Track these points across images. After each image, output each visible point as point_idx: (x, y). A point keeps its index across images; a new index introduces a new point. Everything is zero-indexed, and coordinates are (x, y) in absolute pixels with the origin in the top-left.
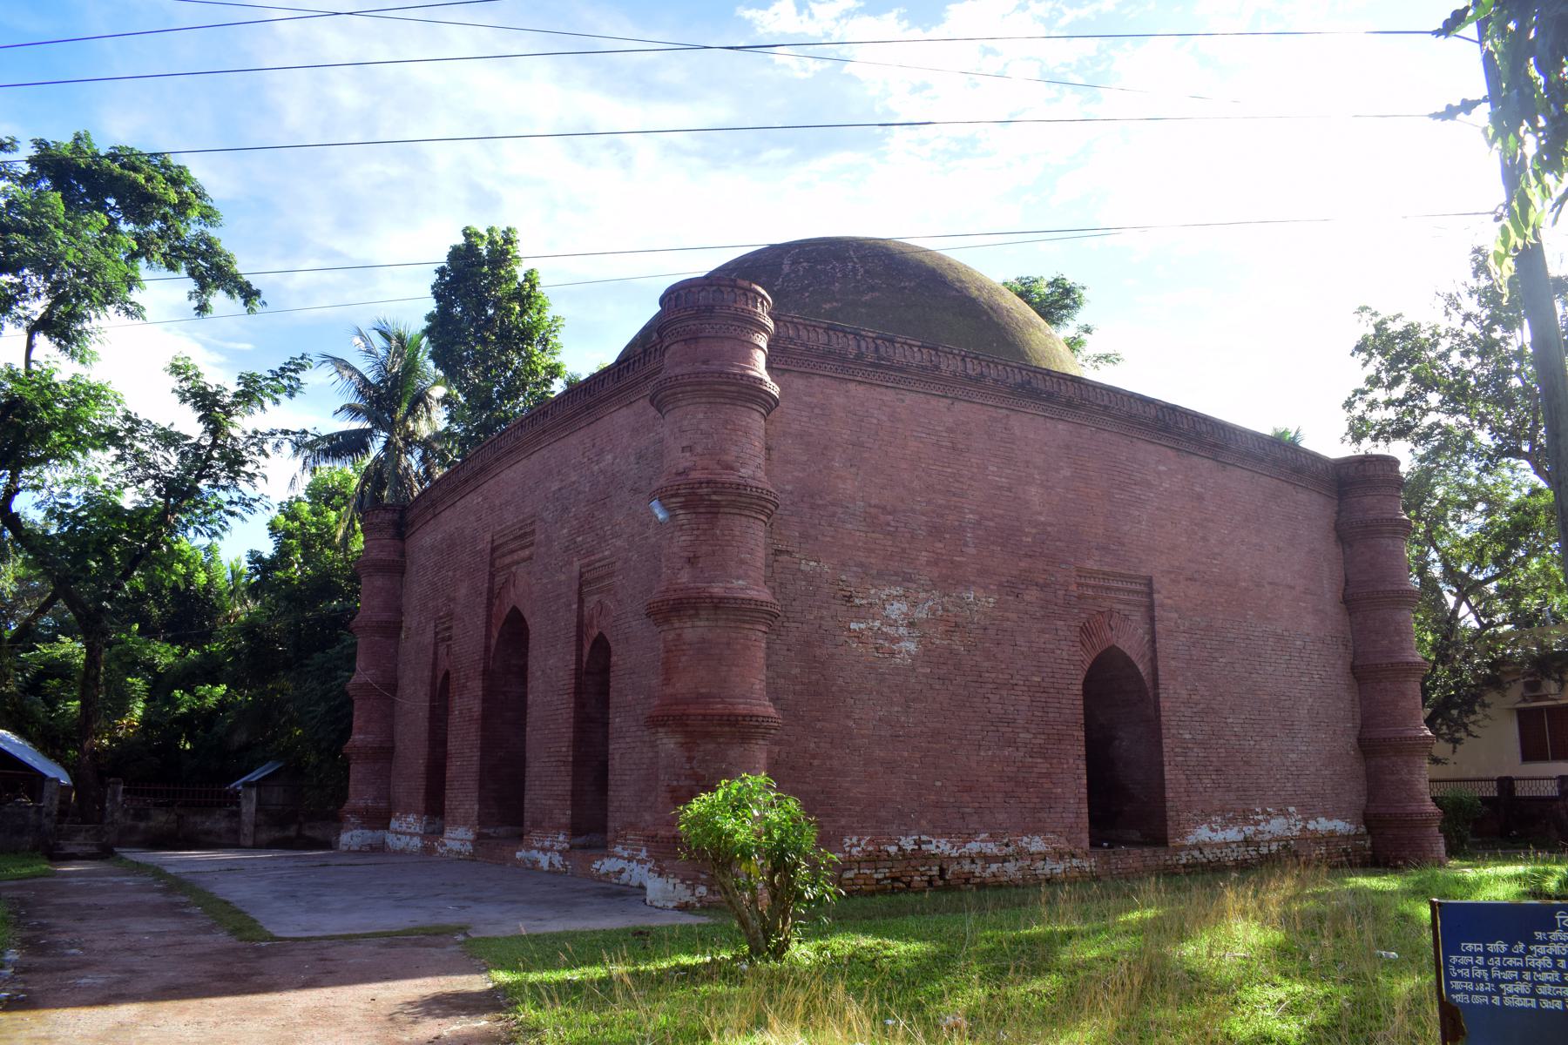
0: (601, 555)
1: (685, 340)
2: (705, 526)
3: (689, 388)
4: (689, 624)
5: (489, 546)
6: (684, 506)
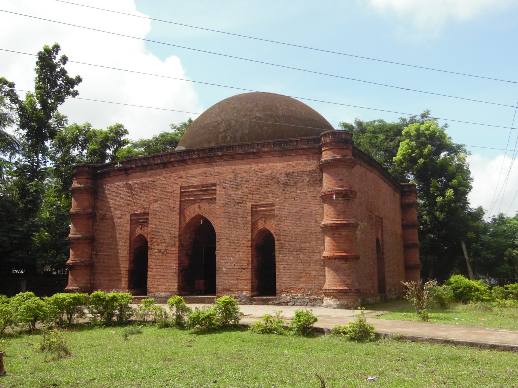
0: (266, 203)
1: (339, 148)
2: (347, 203)
3: (343, 163)
4: (344, 230)
5: (179, 191)
6: (342, 197)
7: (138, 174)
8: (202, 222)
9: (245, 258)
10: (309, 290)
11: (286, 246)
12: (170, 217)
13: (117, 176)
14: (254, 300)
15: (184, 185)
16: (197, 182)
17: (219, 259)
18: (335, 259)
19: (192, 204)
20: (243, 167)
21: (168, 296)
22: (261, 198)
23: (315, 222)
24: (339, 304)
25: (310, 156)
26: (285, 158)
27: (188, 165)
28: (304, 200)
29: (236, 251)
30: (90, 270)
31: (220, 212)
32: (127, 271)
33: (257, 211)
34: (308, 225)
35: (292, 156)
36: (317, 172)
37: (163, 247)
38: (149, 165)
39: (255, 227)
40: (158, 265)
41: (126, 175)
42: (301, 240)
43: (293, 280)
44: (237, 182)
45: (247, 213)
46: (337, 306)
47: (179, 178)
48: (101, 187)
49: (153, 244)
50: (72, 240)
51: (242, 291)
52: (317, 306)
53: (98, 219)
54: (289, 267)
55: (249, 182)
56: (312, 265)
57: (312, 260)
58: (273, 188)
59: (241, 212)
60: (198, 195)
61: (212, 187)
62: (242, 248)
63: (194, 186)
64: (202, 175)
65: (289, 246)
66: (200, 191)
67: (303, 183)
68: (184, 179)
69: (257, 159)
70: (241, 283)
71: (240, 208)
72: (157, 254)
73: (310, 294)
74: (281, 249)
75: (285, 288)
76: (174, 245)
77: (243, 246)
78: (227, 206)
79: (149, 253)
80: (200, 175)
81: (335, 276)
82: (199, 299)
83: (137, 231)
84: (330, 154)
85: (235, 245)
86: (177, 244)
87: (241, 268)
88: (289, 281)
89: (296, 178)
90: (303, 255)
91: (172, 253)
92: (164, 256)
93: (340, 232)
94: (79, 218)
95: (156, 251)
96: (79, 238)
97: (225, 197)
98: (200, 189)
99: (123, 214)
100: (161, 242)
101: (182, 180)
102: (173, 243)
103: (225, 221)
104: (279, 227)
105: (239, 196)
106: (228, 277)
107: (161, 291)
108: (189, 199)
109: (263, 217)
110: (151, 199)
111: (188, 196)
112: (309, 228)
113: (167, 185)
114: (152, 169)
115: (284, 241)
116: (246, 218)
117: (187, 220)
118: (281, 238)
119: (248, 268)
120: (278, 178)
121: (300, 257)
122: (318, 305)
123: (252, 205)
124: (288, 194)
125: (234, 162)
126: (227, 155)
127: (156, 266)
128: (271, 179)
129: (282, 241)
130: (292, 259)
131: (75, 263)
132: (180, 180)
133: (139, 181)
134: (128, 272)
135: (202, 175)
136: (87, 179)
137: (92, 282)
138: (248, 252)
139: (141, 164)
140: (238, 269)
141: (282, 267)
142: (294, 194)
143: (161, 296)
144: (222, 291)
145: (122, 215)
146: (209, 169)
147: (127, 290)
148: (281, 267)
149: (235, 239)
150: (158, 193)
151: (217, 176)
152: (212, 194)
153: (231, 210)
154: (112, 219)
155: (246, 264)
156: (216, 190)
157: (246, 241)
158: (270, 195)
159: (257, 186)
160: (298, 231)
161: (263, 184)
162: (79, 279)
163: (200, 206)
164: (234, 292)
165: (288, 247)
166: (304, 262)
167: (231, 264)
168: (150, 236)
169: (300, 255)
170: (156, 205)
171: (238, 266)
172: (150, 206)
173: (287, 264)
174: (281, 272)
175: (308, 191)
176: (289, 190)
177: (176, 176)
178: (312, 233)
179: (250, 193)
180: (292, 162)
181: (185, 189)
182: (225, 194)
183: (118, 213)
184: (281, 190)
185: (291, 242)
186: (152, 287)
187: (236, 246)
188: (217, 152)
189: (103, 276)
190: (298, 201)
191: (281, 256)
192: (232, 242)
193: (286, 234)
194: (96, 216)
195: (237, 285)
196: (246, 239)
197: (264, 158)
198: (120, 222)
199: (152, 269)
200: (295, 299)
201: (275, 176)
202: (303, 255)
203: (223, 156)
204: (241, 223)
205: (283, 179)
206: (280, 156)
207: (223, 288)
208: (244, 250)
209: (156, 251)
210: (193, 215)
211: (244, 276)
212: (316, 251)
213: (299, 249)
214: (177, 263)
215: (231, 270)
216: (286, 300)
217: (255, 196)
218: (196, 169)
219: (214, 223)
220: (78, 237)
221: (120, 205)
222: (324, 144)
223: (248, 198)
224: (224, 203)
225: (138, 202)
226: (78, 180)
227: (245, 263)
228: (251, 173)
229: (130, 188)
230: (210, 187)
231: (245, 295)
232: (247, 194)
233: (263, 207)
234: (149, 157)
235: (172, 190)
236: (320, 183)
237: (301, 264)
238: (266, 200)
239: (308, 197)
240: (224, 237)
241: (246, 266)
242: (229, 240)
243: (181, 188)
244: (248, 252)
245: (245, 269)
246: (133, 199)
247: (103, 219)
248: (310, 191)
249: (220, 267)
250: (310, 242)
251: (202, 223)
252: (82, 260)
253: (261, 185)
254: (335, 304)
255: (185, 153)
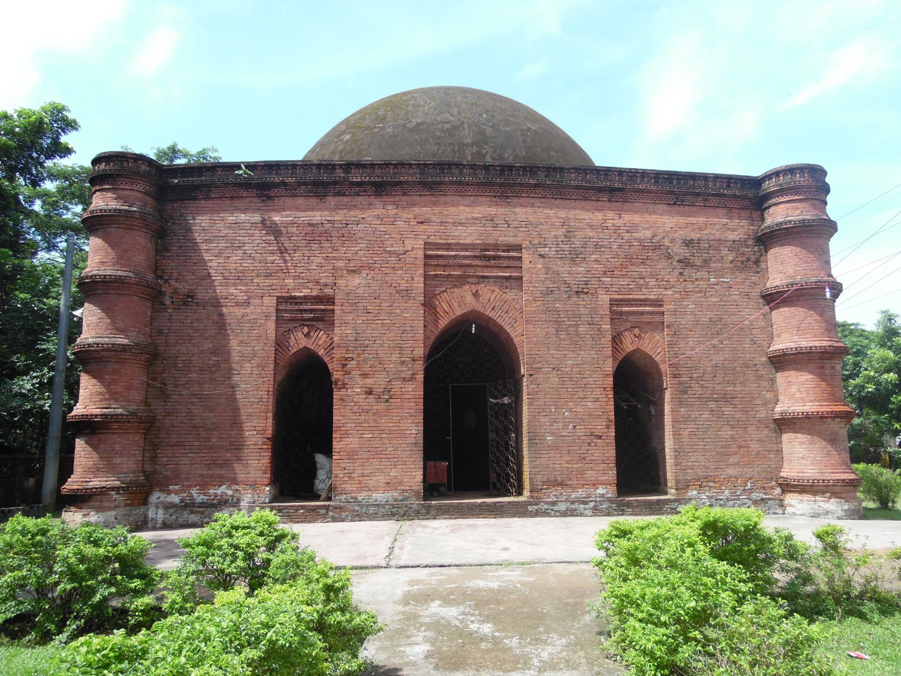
5: (420, 254)
7: (300, 201)
8: (473, 329)
9: (601, 413)
10: (747, 481)
11: (694, 389)
12: (398, 311)
13: (232, 198)
14: (629, 504)
15: (433, 239)
16: (470, 238)
17: (535, 414)
18: (834, 418)
19: (455, 286)
20: (587, 217)
21: (395, 500)
22: (631, 287)
23: (752, 342)
24: (849, 509)
25: (734, 210)
26: (682, 209)
27: (446, 195)
28: (725, 298)
29: (577, 396)
30: (143, 436)
31: (534, 309)
32: (268, 438)
33: (621, 313)
34: (738, 349)
35: (695, 209)
36: (749, 245)
37: (378, 382)
38: (335, 183)
39: (617, 347)
40: (365, 425)
41: (263, 201)
42: (726, 379)
43: (712, 460)
44: (573, 246)
45: (600, 316)
46: (844, 513)
47: (422, 223)
48: (177, 222)
49: (348, 373)
50: (103, 351)
51: (595, 485)
52: (769, 513)
53: (168, 302)
54: (701, 433)
55: (603, 249)
56: (751, 429)
57: (750, 419)
58: (659, 266)
59: (587, 312)
60: (472, 266)
61: (508, 251)
62: (591, 390)
63: (462, 244)
64: (483, 222)
65: (700, 389)
66: (476, 257)
67: (721, 263)
68: (435, 227)
69: (619, 204)
70: (591, 469)
71: (584, 303)
72: (361, 399)
73: (749, 489)
74: (682, 396)
75: (694, 477)
76: (412, 379)
77: (594, 386)
78: (550, 298)
79: (335, 397)
80: (477, 222)
81: (832, 453)
82: (487, 505)
83: (292, 337)
84: (807, 209)
85: (574, 383)
86: (420, 377)
87: (592, 434)
88: (703, 463)
89: (706, 251)
90: (731, 409)
91: (408, 397)
92: (384, 404)
93: (833, 365)
94: (121, 294)
95: (358, 390)
96: (124, 348)
97: (546, 276)
98: (477, 254)
99: (253, 294)
100: (374, 369)
101: (427, 227)
102: (407, 374)
103: (546, 330)
104: (677, 349)
105: (580, 277)
106: (559, 455)
107: (376, 490)
108: (449, 275)
109: (635, 327)
110: (341, 264)
111: (444, 266)
112: (739, 355)
113: (386, 236)
114: (344, 195)
115: (688, 379)
116: (599, 326)
117: (443, 323)
118: (680, 372)
119: (609, 434)
120: (668, 248)
121: (725, 413)
122: (772, 511)
123: (611, 300)
124: (690, 283)
125: (564, 202)
126: (548, 186)
127: (358, 428)
128: (653, 248)
129: (685, 379)
130: (708, 416)
131: (112, 415)
132: (423, 227)
133: (304, 217)
134: (270, 443)
135: (483, 222)
136: (146, 193)
137: (148, 467)
138: (606, 400)
139: (310, 177)
140: (583, 438)
141: (686, 433)
142: (703, 284)
143: (376, 500)
144: (545, 487)
145: (250, 298)
146: (501, 211)
147: (268, 489)
148: (684, 433)
149: (575, 370)
150: (359, 252)
151: (521, 229)
152: (509, 267)
153: (560, 306)
154: (216, 304)
155: (603, 427)
156: (520, 259)
157: (600, 376)
158: (652, 282)
159: (621, 260)
160: (717, 358)
161: (634, 257)
162: (118, 460)
163: (477, 291)
164: (574, 488)
165: (698, 393)
166: (733, 423)
167: (566, 426)
168: (338, 353)
169: (725, 409)
170: (356, 280)
171: (583, 431)
172: (336, 281)
173: (696, 426)
174: (685, 443)
175: (733, 280)
176: (693, 275)
177: (411, 216)
178: (747, 366)
179: (605, 274)
180: (696, 219)
181: (438, 249)
182: (543, 270)
183: (235, 291)
184: (676, 273)
185: (703, 382)
186: (347, 479)
187: (576, 386)
188: (525, 175)
189: (187, 451)
190: (714, 300)
191: (683, 409)
192: (565, 376)
193: (692, 365)
194: (161, 293)
195: (581, 472)
196: (602, 372)
197: (634, 204)
198: (243, 316)
199: (347, 434)
200: (721, 500)
201: (661, 243)
202: (731, 409)
203: (539, 187)
204: (589, 336)
205: (679, 250)
206: (672, 203)
207: (548, 481)
208: (598, 396)
209: (358, 390)
210: (459, 312)
211: (598, 451)
212: (758, 402)
213: (722, 396)
214: (422, 421)
215: (567, 438)
216: (701, 502)
217: (616, 279)
218: (466, 206)
219: (516, 333)
220: (123, 345)
221: (243, 272)
222: (793, 189)
223: (601, 283)
224: (544, 289)
225: (300, 270)
226: (121, 192)
227: (600, 424)
228: (605, 231)
229: (275, 231)
230: (503, 251)
231: (602, 495)
232: (598, 276)
233: (636, 305)
234: (334, 165)
235: (402, 248)
236: (755, 266)
237: (728, 426)
238: (643, 290)
239: (732, 293)
240: (547, 366)
241: (603, 431)
242: (559, 372)
243: (426, 247)
244: (606, 400)
245: (601, 436)
246: (285, 261)
247: (185, 304)
248: (737, 280)
249: (538, 431)
250: (743, 383)
251: (473, 332)
252: (132, 407)
253: (630, 258)
254: (840, 509)
255: (438, 167)
